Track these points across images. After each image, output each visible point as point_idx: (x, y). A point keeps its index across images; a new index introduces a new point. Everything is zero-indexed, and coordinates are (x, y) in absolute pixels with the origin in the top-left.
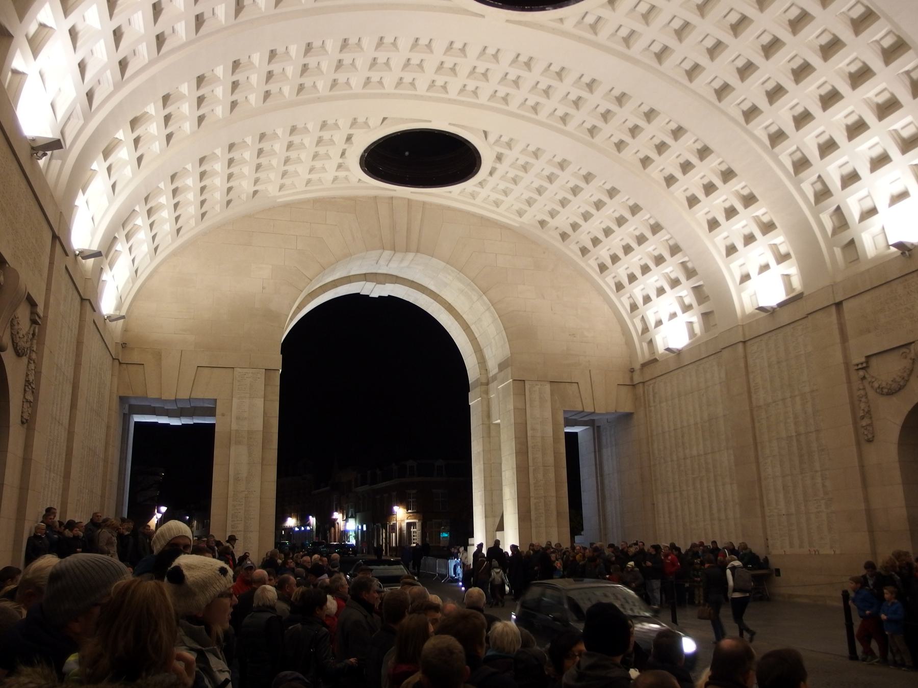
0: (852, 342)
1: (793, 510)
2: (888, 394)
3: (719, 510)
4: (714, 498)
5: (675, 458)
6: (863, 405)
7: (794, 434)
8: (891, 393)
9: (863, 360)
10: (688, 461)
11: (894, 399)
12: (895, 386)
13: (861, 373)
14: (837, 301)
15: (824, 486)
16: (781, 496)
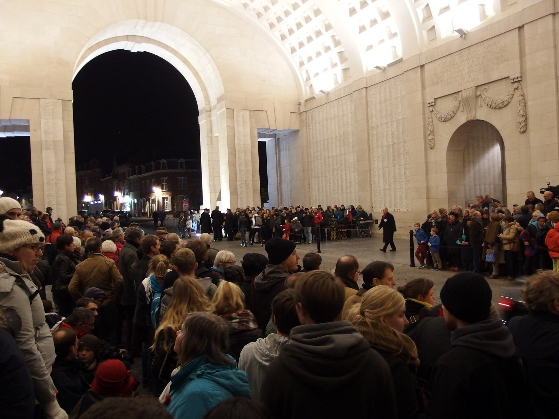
0: (427, 90)
1: (387, 188)
2: (444, 121)
3: (347, 188)
4: (344, 180)
5: (323, 157)
6: (430, 128)
7: (391, 144)
8: (446, 121)
9: (433, 100)
10: (330, 159)
11: (447, 124)
12: (449, 117)
13: (431, 108)
14: (421, 64)
15: (405, 173)
16: (381, 179)
